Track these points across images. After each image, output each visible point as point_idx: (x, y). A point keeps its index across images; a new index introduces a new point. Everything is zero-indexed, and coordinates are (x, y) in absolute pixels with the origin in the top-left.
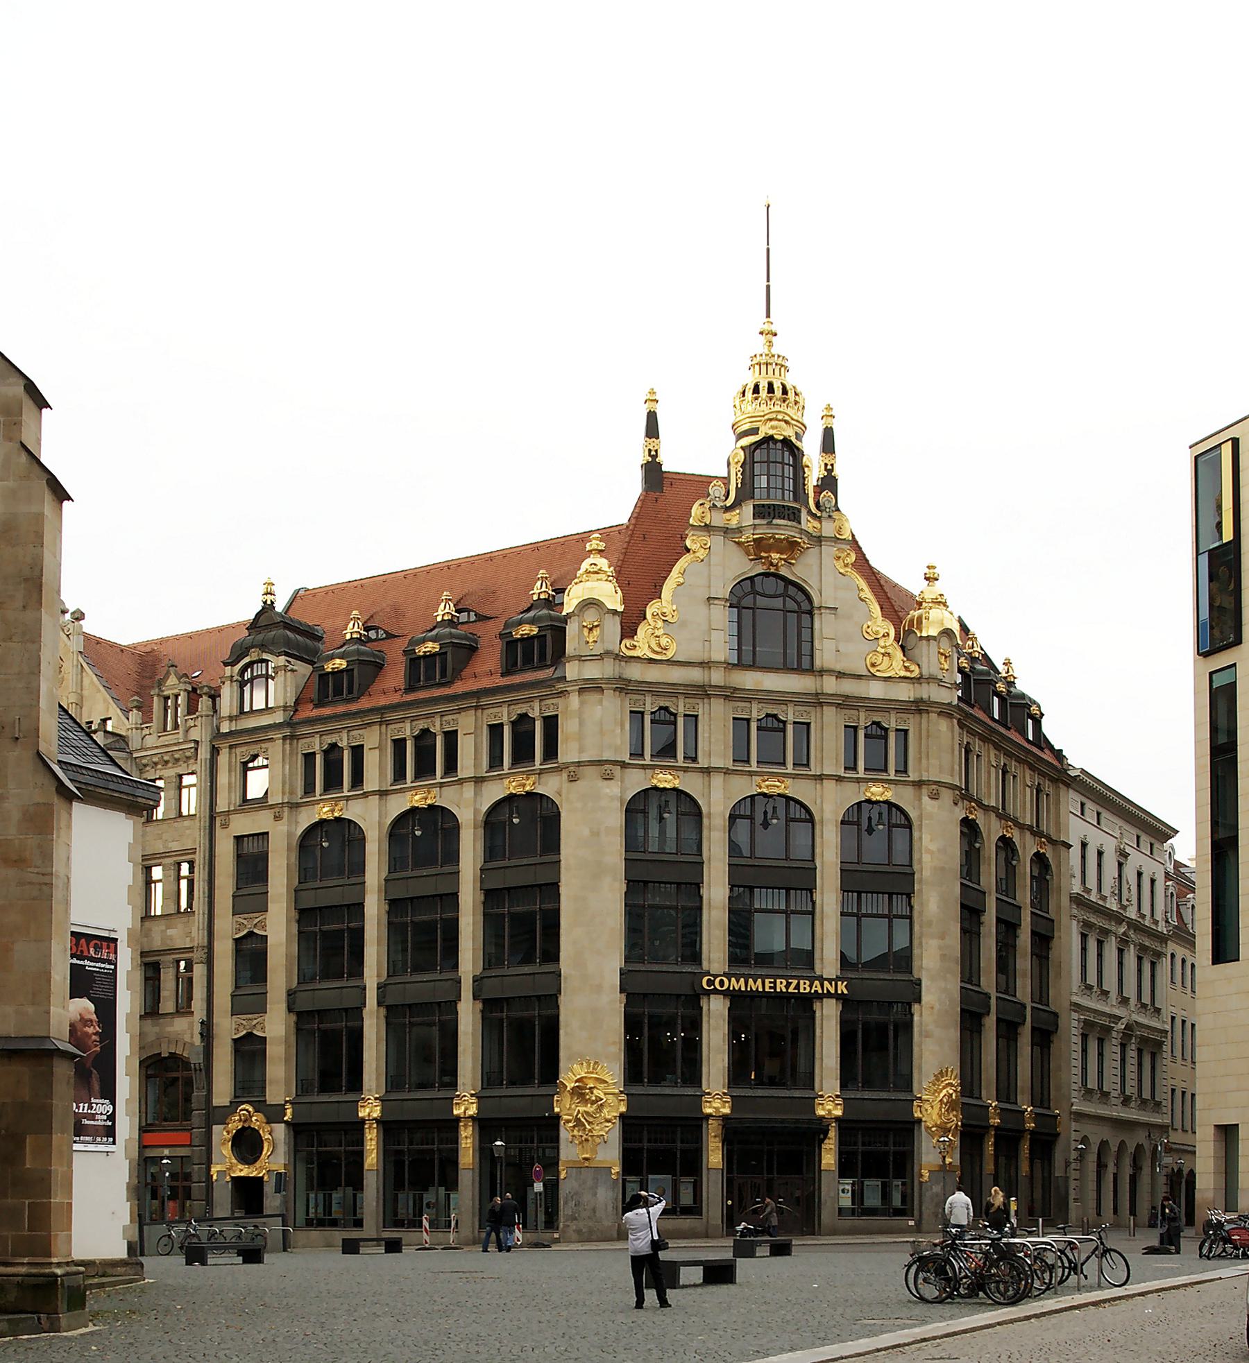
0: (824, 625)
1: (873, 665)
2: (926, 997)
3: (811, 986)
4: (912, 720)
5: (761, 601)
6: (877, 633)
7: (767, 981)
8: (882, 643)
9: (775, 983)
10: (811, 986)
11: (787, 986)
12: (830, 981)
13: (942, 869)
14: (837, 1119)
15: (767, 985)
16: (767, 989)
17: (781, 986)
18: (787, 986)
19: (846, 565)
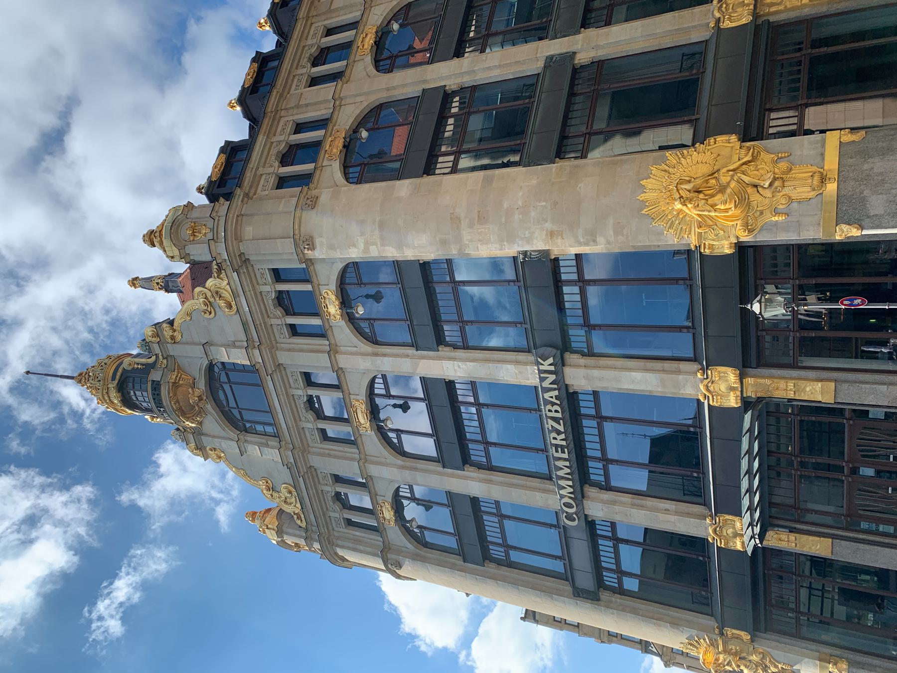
0: (223, 355)
1: (230, 307)
2: (539, 245)
3: (553, 404)
4: (259, 266)
5: (232, 404)
6: (205, 304)
7: (556, 455)
8: (212, 300)
9: (557, 446)
10: (553, 404)
11: (559, 433)
12: (542, 380)
13: (382, 226)
14: (742, 377)
15: (559, 455)
16: (566, 456)
17: (560, 440)
18: (559, 433)
19: (174, 331)
